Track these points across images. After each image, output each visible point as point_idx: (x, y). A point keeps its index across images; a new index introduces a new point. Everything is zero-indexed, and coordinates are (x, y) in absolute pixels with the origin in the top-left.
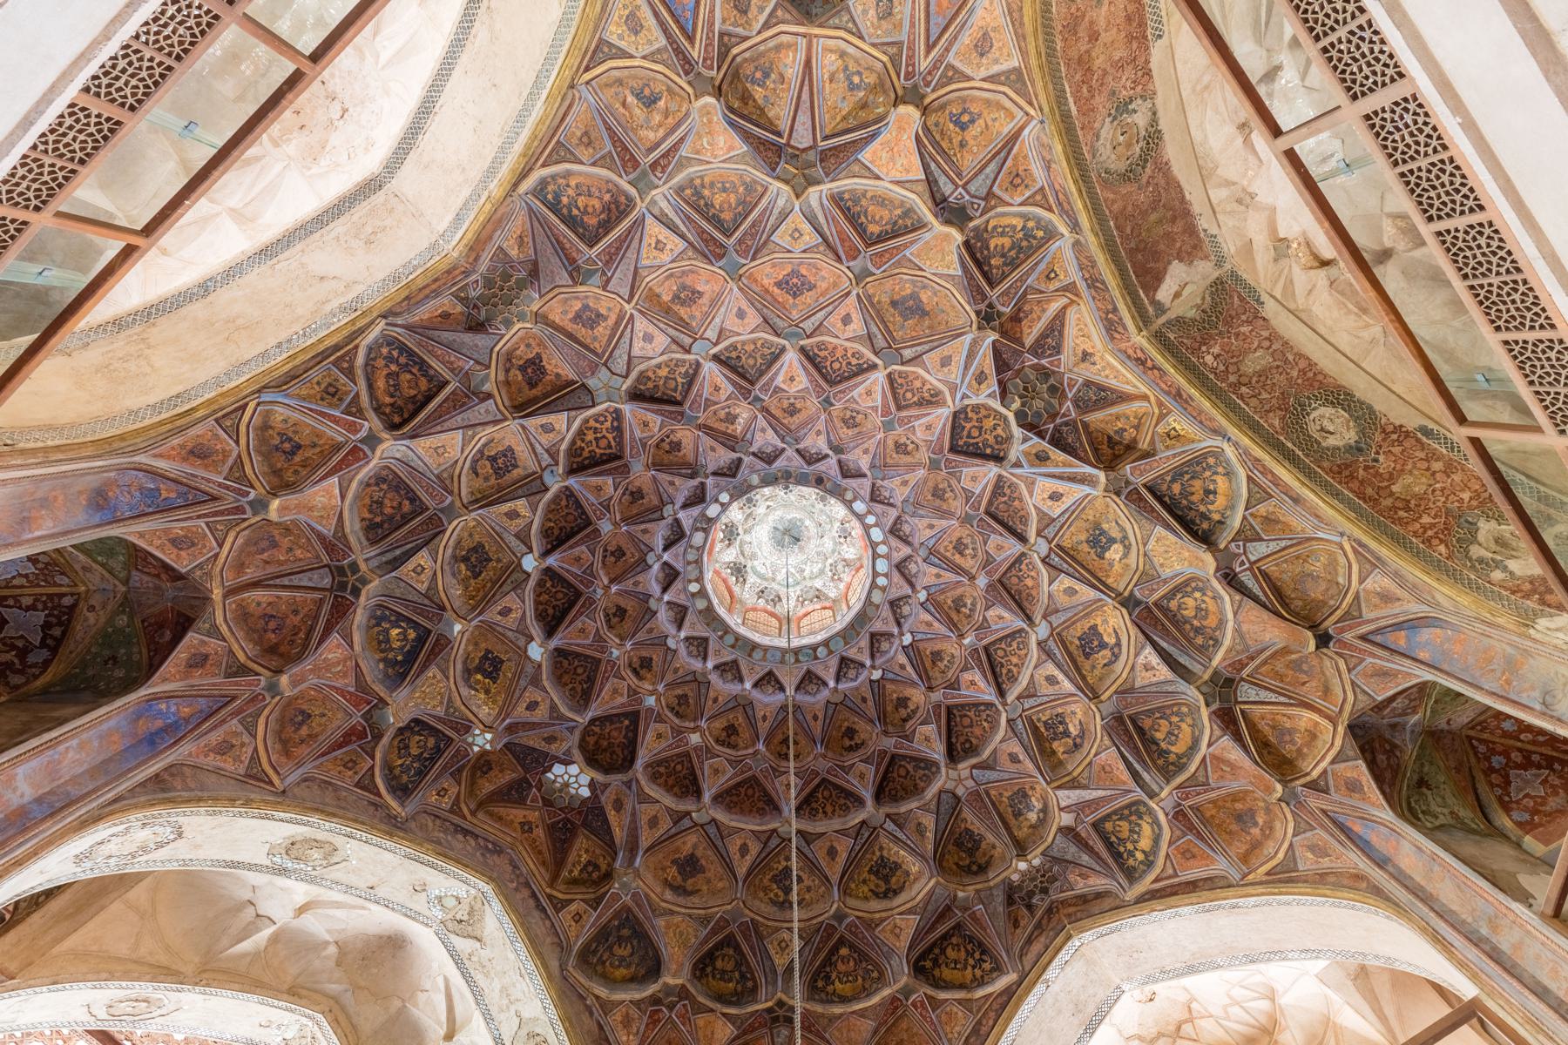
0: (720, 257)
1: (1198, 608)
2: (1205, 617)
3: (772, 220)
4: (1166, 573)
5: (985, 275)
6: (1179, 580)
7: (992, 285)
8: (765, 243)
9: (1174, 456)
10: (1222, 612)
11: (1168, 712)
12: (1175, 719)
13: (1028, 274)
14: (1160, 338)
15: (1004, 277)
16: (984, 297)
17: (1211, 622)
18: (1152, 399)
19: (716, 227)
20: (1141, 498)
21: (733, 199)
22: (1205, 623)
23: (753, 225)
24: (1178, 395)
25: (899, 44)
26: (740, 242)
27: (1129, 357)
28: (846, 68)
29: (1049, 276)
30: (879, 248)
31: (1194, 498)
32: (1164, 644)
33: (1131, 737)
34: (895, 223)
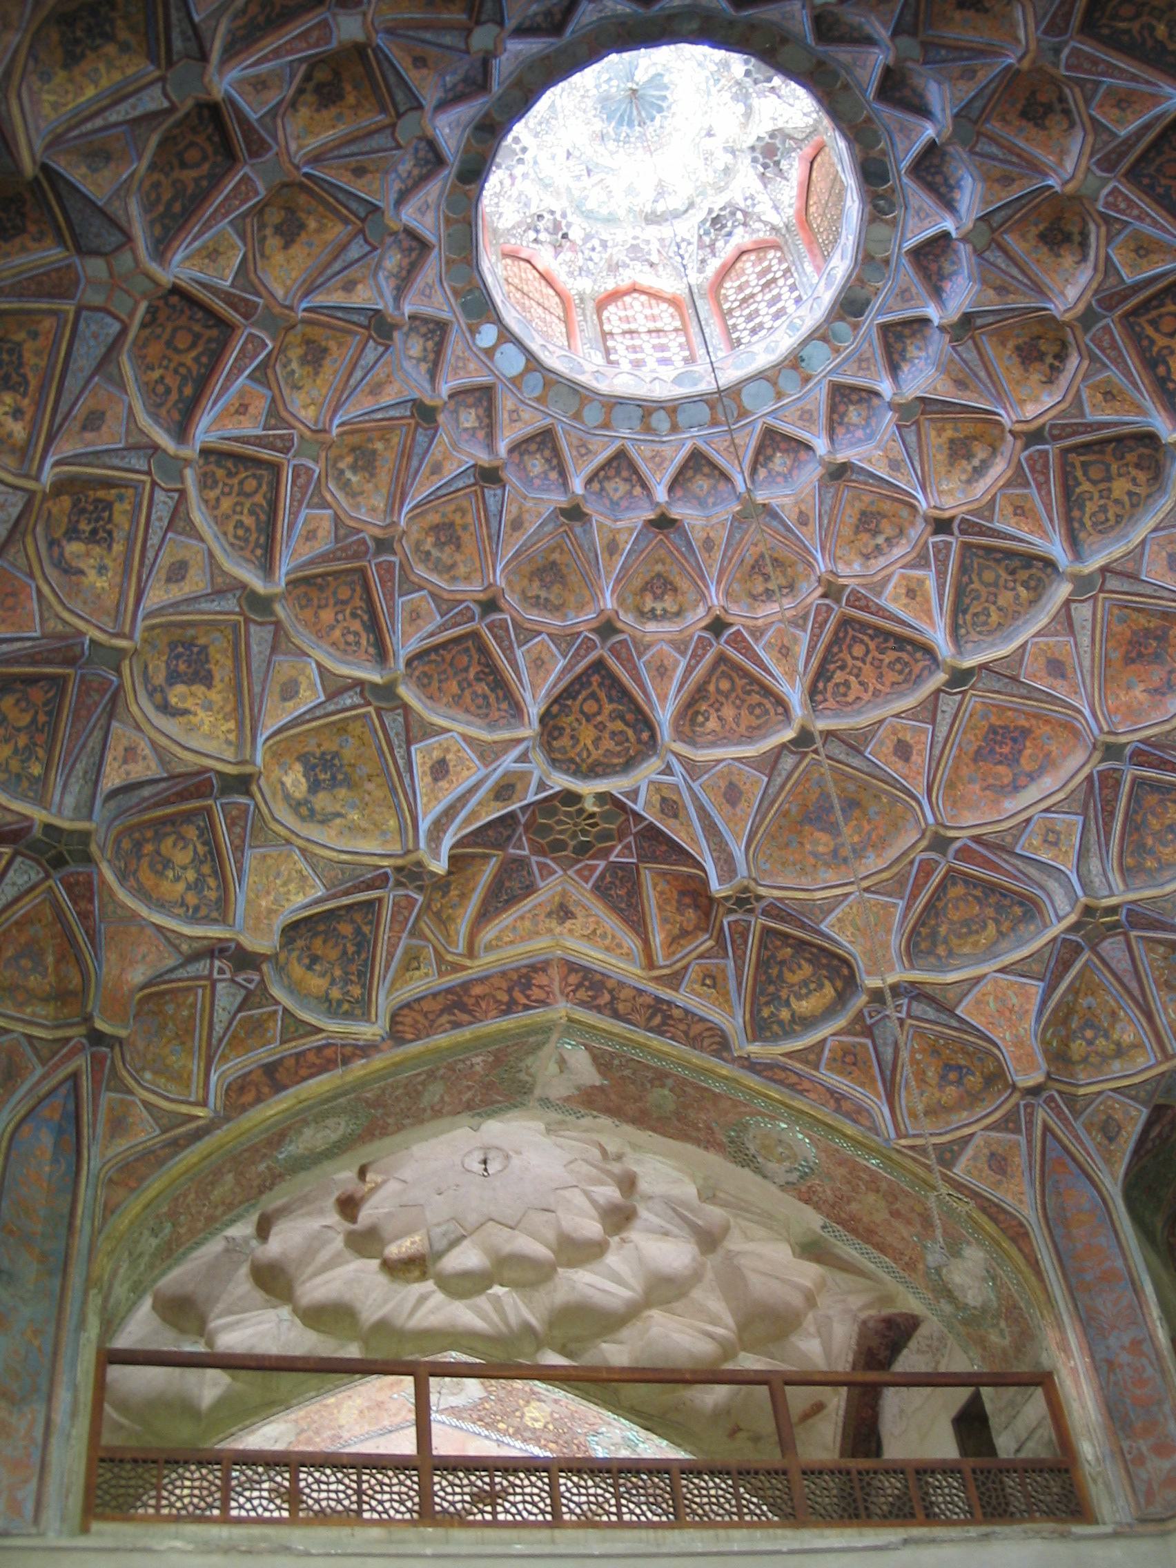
0: (1137, 753)
1: (168, 863)
2: (152, 866)
3: (1093, 837)
4: (251, 858)
5: (787, 936)
6: (231, 868)
7: (767, 931)
8: (1085, 807)
9: (391, 955)
10: (161, 905)
11: (41, 738)
12: (22, 740)
13: (739, 970)
14: (545, 1030)
15: (762, 945)
16: (765, 913)
17: (146, 876)
18: (468, 963)
19: (1159, 781)
20: (370, 886)
21: (1154, 823)
22: (145, 862)
23: (1112, 814)
24: (458, 1003)
25: (1077, 1114)
26: (1118, 783)
27: (534, 968)
28: (1106, 1036)
29: (712, 980)
30: (936, 879)
31: (318, 942)
32: (146, 792)
33: (34, 663)
34: (937, 915)
